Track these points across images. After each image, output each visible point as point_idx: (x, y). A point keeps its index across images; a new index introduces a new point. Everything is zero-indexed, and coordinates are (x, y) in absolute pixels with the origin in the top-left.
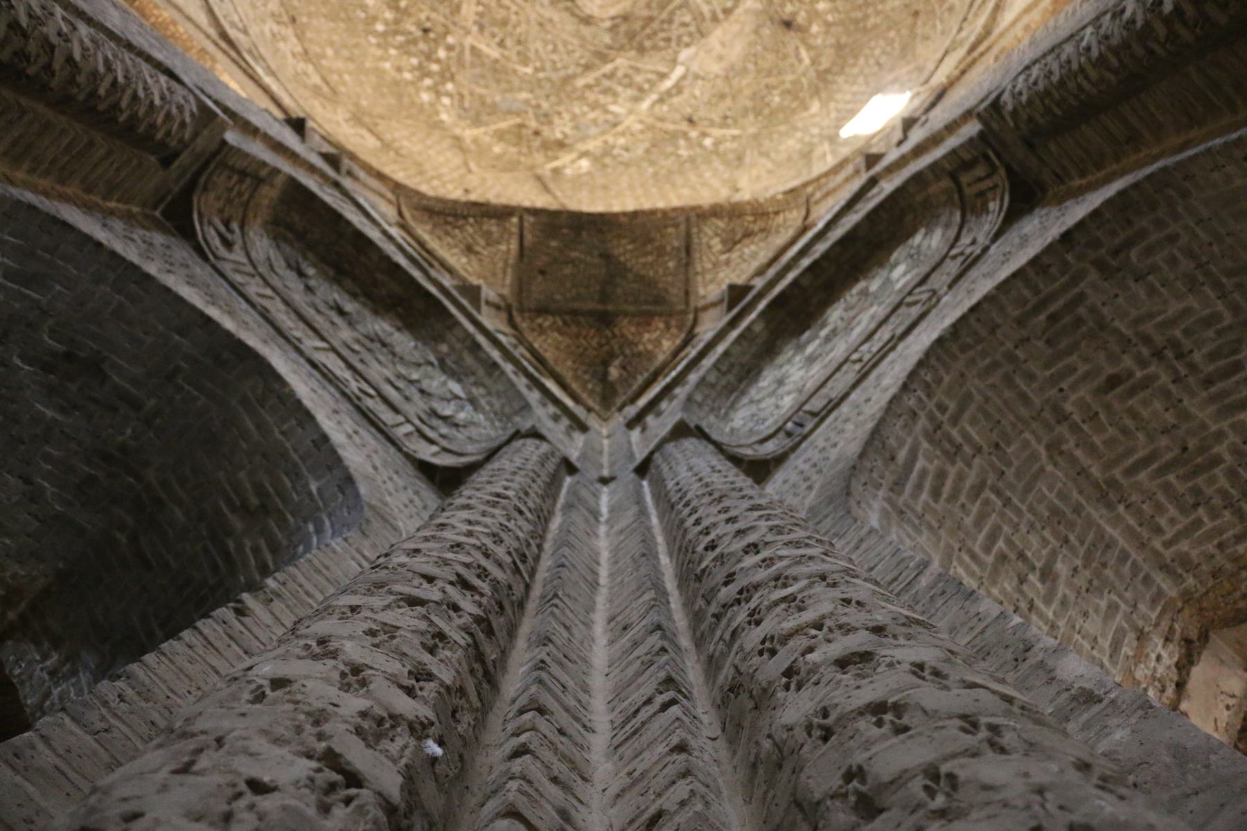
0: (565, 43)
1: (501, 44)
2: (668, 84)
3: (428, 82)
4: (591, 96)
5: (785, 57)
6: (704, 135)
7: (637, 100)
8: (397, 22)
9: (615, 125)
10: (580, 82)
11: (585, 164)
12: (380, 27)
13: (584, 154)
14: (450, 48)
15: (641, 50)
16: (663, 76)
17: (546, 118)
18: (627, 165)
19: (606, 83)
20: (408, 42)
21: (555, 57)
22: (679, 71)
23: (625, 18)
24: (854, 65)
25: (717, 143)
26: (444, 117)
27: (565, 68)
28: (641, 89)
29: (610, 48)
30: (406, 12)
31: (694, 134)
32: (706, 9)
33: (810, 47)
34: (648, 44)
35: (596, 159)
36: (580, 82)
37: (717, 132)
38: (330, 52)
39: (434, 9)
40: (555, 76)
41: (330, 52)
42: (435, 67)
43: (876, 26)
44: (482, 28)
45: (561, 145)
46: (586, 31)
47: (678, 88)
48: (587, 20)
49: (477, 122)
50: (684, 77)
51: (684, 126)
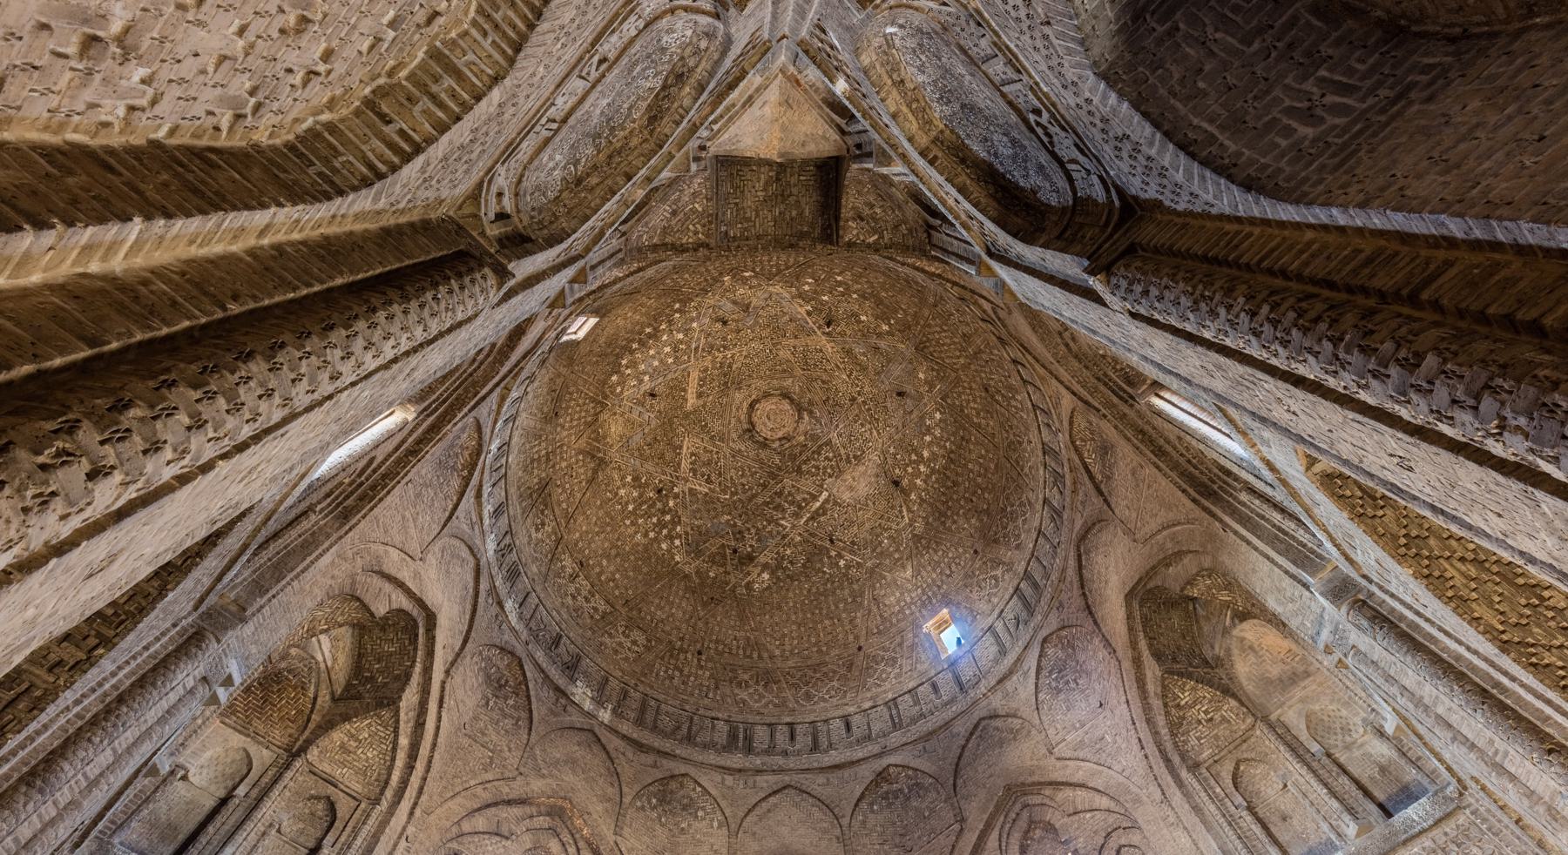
0: (749, 467)
1: (709, 481)
2: (818, 504)
3: (665, 532)
4: (767, 511)
5: (893, 507)
6: (840, 556)
7: (797, 515)
8: (641, 496)
9: (784, 537)
10: (760, 500)
11: (766, 576)
12: (631, 508)
13: (765, 567)
14: (676, 496)
15: (799, 471)
16: (815, 498)
17: (739, 535)
18: (791, 578)
19: (778, 500)
20: (651, 507)
21: (743, 481)
22: (825, 495)
23: (787, 438)
24: (936, 551)
25: (848, 567)
26: (677, 558)
27: (751, 489)
28: (800, 507)
29: (780, 469)
30: (647, 485)
31: (833, 553)
32: (843, 451)
33: (909, 510)
34: (804, 468)
35: (772, 573)
36: (760, 500)
37: (848, 557)
38: (605, 563)
39: (664, 473)
40: (743, 497)
41: (605, 563)
42: (668, 517)
43: (949, 529)
44: (694, 471)
45: (751, 558)
46: (763, 454)
47: (822, 510)
48: (764, 444)
49: (698, 553)
50: (827, 501)
51: (827, 544)
